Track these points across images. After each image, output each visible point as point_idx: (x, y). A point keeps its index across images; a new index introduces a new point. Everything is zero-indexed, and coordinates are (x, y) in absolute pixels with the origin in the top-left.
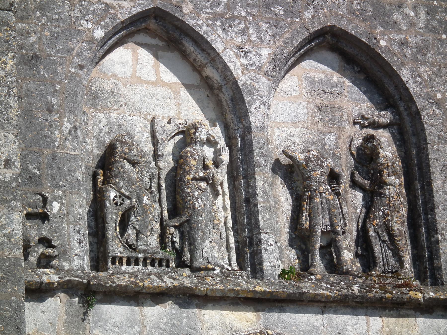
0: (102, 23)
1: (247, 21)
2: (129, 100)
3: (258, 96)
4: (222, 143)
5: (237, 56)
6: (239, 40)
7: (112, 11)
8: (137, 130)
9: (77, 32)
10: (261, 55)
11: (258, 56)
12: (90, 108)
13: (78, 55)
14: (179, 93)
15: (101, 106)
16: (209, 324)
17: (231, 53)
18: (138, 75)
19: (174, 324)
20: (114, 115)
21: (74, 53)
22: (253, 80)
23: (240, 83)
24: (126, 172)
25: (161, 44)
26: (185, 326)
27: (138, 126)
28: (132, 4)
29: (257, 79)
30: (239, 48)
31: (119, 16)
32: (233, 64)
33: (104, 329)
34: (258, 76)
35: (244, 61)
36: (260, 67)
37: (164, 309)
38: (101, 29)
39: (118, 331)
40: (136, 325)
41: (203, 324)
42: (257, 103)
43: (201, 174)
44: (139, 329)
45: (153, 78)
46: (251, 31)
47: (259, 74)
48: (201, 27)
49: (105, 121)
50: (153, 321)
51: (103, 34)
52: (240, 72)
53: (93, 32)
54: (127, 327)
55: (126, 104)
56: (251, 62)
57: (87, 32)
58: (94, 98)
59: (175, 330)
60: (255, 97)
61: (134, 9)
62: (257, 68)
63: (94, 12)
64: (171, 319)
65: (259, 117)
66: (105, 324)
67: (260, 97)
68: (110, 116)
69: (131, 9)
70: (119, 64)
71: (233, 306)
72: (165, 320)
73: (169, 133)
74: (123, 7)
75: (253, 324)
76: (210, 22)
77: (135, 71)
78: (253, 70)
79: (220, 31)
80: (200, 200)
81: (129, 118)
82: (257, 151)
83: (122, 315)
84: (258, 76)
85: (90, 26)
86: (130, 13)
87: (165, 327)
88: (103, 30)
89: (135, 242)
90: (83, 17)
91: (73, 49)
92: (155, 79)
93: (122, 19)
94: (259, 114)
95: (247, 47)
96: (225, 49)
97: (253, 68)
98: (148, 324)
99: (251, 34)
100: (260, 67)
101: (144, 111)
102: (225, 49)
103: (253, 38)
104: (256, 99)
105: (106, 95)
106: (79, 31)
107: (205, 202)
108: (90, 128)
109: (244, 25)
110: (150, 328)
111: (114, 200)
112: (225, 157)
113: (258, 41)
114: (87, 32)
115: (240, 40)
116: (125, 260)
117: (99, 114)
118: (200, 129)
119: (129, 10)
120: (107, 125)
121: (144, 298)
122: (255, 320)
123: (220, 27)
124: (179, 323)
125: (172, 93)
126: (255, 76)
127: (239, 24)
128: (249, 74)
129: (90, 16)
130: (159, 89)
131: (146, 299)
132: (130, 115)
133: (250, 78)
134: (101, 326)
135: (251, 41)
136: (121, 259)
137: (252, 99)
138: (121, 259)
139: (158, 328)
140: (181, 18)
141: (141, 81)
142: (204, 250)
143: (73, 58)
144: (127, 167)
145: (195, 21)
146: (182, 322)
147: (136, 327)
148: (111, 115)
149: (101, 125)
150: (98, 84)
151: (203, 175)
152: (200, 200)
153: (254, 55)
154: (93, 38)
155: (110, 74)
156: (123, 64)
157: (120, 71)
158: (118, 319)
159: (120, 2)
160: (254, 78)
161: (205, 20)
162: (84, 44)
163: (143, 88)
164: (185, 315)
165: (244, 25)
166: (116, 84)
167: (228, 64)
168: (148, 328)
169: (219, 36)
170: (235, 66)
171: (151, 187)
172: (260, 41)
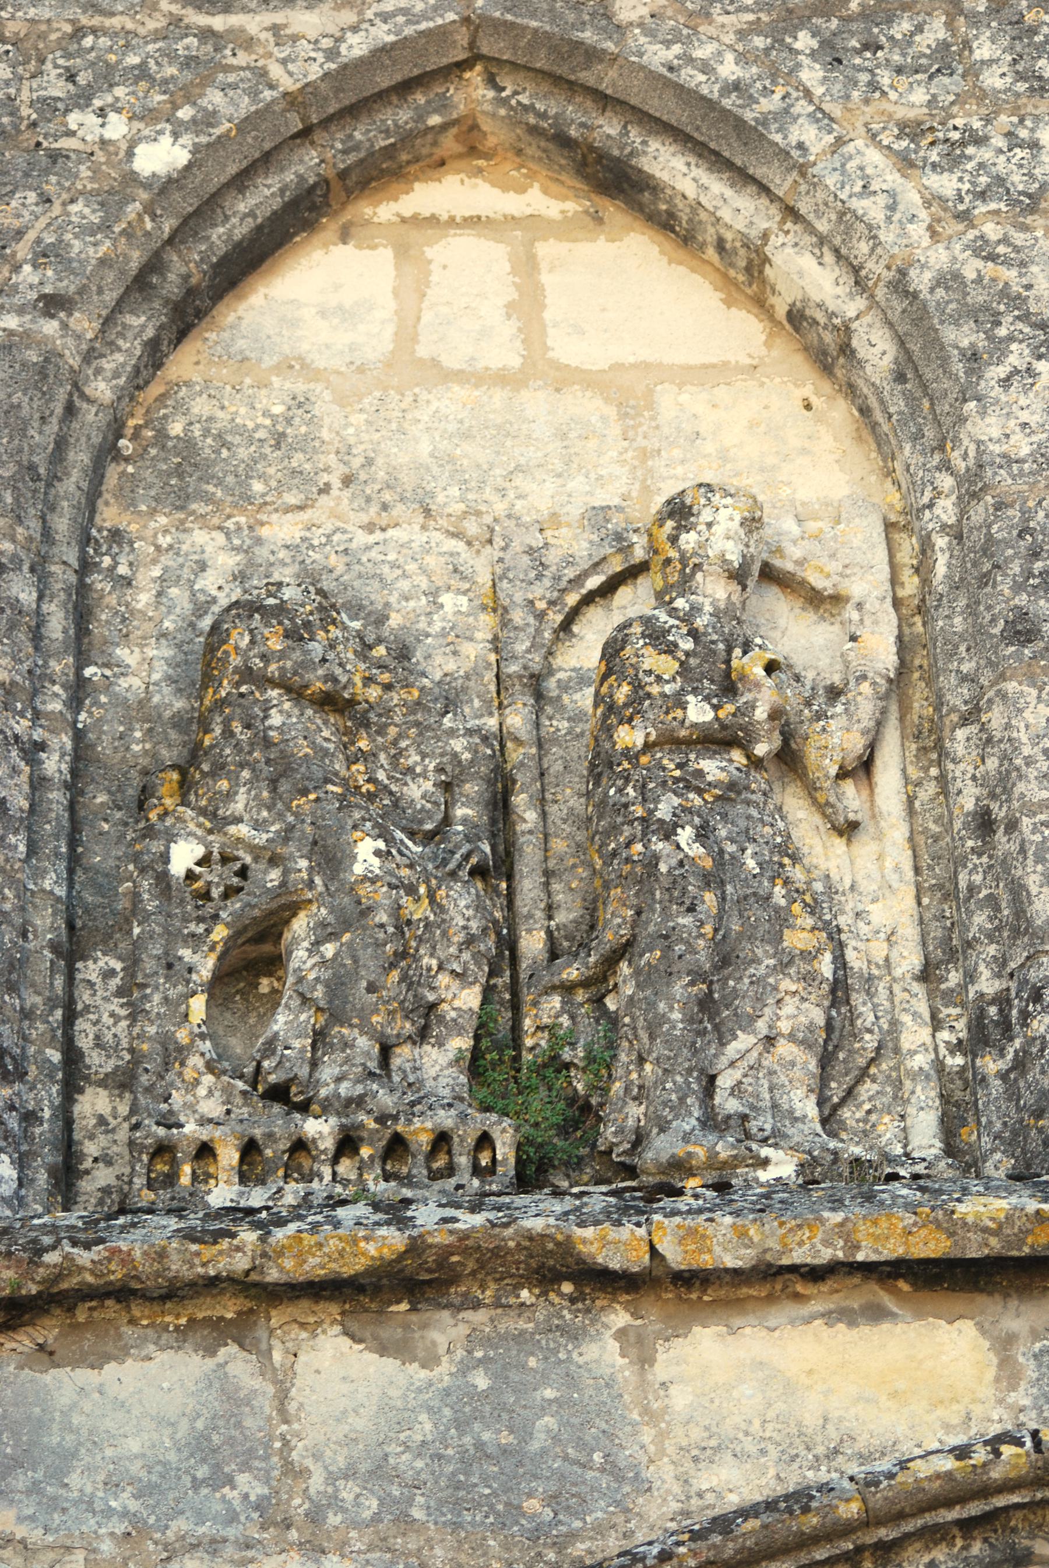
0: (185, 113)
1: (961, 12)
2: (369, 462)
3: (1020, 325)
4: (868, 585)
5: (906, 163)
6: (914, 98)
7: (243, 59)
8: (404, 585)
9: (45, 161)
10: (1034, 146)
11: (1019, 153)
12: (153, 512)
13: (43, 255)
14: (650, 406)
15: (209, 499)
16: (696, 1434)
17: (874, 157)
18: (423, 351)
19: (479, 1445)
20: (281, 530)
21: (22, 250)
22: (992, 257)
23: (921, 280)
24: (268, 744)
25: (542, 200)
26: (544, 1452)
27: (411, 567)
28: (349, 17)
29: (1017, 249)
30: (911, 130)
31: (276, 71)
32: (882, 200)
33: (54, 1504)
34: (1019, 238)
35: (946, 184)
36: (1029, 196)
37: (424, 1374)
38: (176, 135)
39: (133, 1505)
40: (245, 1467)
41: (662, 1436)
42: (1017, 356)
43: (698, 712)
44: (258, 1490)
45: (503, 353)
46: (983, 50)
47: (1025, 228)
48: (706, 68)
49: (228, 561)
50: (351, 1441)
51: (181, 157)
52: (918, 231)
53: (130, 154)
54: (187, 1480)
55: (347, 481)
56: (984, 180)
57: (100, 157)
58: (179, 472)
59: (486, 1480)
60: (1002, 332)
61: (352, 39)
62: (1013, 203)
63: (142, 72)
64: (461, 1424)
65: (1024, 416)
66: (58, 1475)
67: (1035, 326)
68: (259, 541)
69: (339, 40)
70: (323, 314)
71: (852, 1323)
72: (425, 1427)
73: (570, 573)
74: (295, 38)
75: (977, 1410)
76: (760, 42)
77: (407, 333)
78: (997, 212)
79: (811, 75)
80: (685, 835)
81: (362, 538)
82: (1015, 568)
83: (161, 1421)
84: (1019, 238)
85: (117, 128)
86: (332, 54)
87: (419, 1464)
88: (187, 139)
89: (304, 1072)
90: (82, 99)
91: (20, 234)
92: (516, 362)
93: (288, 84)
94: (1023, 401)
95: (959, 122)
96: (840, 142)
97: (993, 206)
98: (317, 1457)
99: (982, 62)
100: (1029, 196)
101: (449, 499)
102: (840, 142)
103: (993, 80)
104: (1011, 339)
105: (243, 453)
106: (55, 156)
107: (730, 848)
108: (143, 599)
109: (942, 34)
110: (331, 1478)
111: (190, 876)
112: (881, 650)
113: (1021, 87)
114: (100, 157)
115: (919, 96)
116: (229, 1156)
117: (200, 536)
118: (706, 515)
119: (326, 43)
120: (240, 577)
121: (303, 1325)
122: (987, 1392)
123: (813, 54)
124: (506, 1438)
125: (612, 411)
126: (1005, 240)
127: (919, 29)
128: (971, 234)
129: (120, 91)
130: (536, 402)
131: (312, 1329)
132: (370, 528)
133: (976, 253)
134: (35, 1489)
135: (982, 95)
136: (205, 1151)
137: (990, 337)
138: (205, 1151)
139: (381, 1471)
140: (610, 46)
141: (440, 374)
142: (725, 1081)
143: (17, 268)
144: (276, 719)
145: (677, 49)
146: (525, 1433)
147: (243, 1479)
148: (264, 532)
149: (208, 582)
150: (201, 407)
151: (709, 716)
152: (685, 835)
153: (1000, 151)
154: (132, 178)
155: (268, 362)
156: (347, 315)
157: (320, 340)
158: (134, 1446)
159: (278, 18)
160: (1001, 249)
161: (729, 38)
162: (74, 208)
163: (451, 403)
164: (549, 1393)
165: (942, 34)
166: (301, 403)
167: (856, 204)
168: (317, 1482)
169: (808, 94)
170: (892, 208)
171: (447, 820)
172: (1032, 89)
